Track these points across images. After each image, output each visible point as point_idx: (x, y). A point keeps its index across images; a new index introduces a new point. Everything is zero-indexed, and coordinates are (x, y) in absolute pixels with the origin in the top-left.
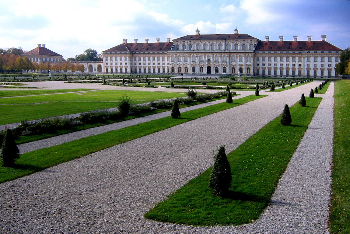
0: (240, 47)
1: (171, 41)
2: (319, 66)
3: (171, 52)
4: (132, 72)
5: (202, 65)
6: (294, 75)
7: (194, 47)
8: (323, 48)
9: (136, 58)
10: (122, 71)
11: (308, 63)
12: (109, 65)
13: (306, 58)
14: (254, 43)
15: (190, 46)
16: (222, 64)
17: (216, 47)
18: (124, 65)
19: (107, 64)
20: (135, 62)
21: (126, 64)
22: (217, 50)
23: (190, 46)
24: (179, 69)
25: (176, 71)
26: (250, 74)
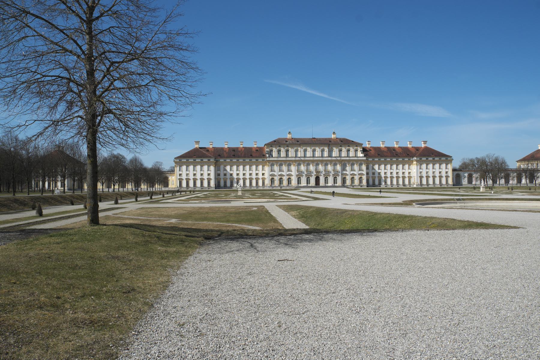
0: (344, 154)
1: (262, 145)
2: (431, 174)
3: (268, 159)
4: (218, 186)
5: (309, 175)
6: (404, 184)
7: (292, 153)
8: (432, 154)
9: (220, 166)
10: (181, 185)
11: (421, 170)
12: (184, 177)
13: (419, 166)
14: (360, 149)
15: (287, 151)
16: (333, 174)
17: (318, 153)
18: (205, 177)
19: (180, 175)
20: (219, 172)
21: (209, 175)
22: (319, 157)
23: (287, 151)
24: (281, 180)
25: (277, 183)
26: (363, 185)
